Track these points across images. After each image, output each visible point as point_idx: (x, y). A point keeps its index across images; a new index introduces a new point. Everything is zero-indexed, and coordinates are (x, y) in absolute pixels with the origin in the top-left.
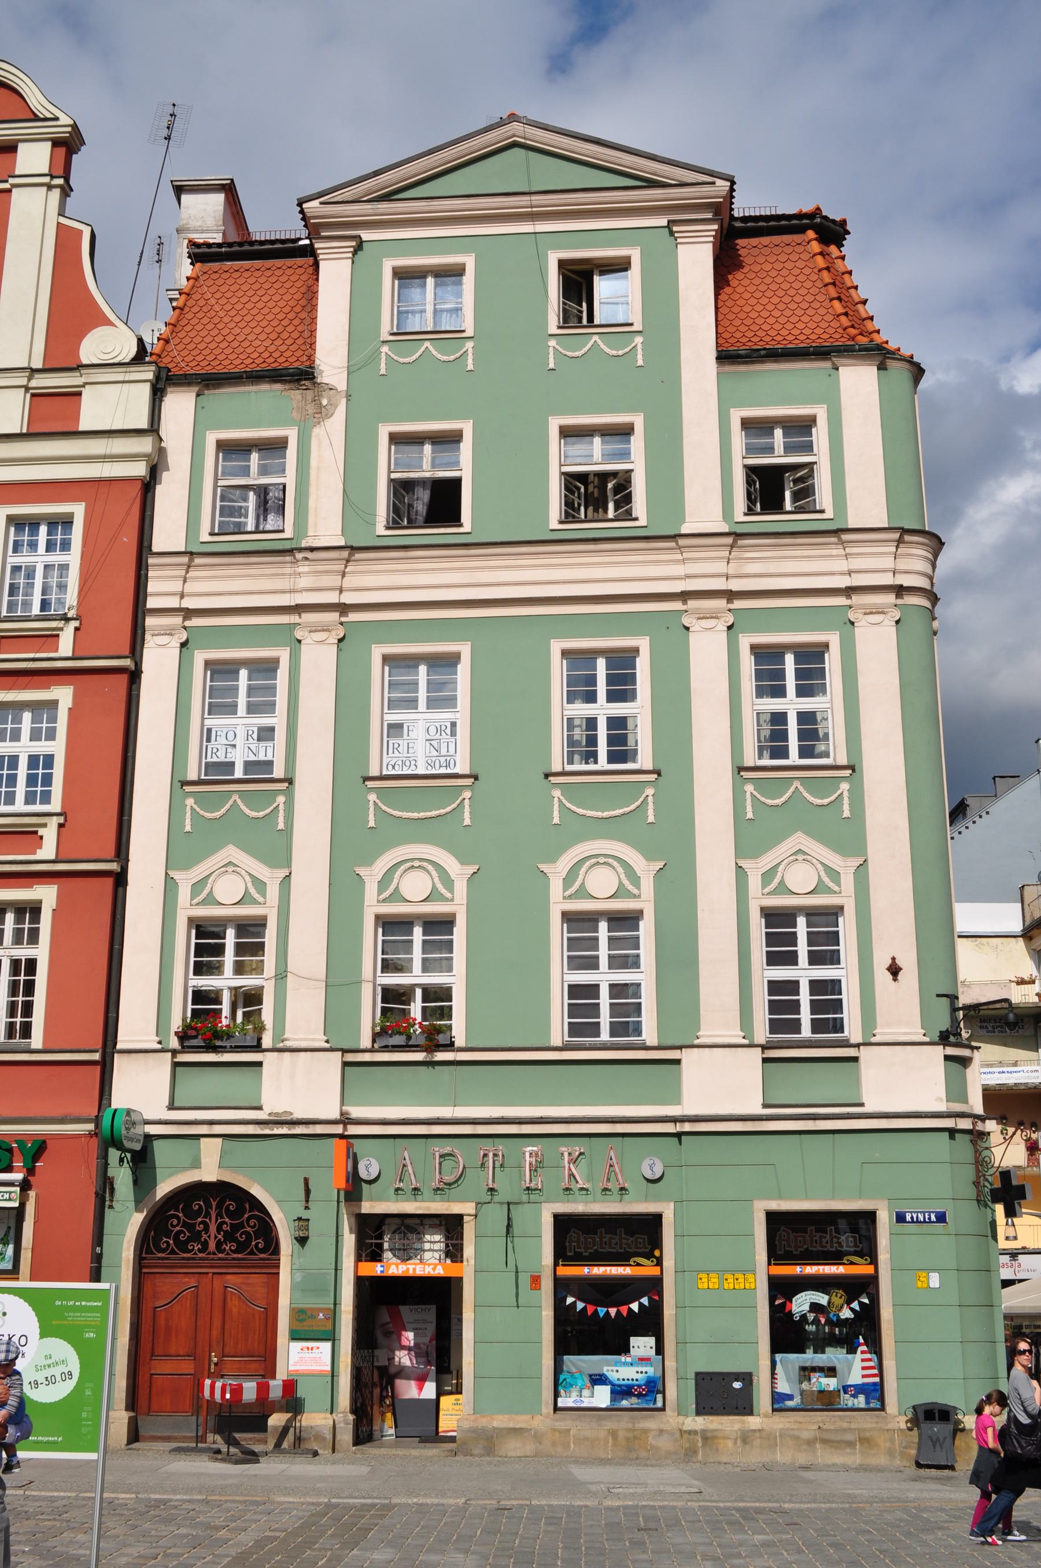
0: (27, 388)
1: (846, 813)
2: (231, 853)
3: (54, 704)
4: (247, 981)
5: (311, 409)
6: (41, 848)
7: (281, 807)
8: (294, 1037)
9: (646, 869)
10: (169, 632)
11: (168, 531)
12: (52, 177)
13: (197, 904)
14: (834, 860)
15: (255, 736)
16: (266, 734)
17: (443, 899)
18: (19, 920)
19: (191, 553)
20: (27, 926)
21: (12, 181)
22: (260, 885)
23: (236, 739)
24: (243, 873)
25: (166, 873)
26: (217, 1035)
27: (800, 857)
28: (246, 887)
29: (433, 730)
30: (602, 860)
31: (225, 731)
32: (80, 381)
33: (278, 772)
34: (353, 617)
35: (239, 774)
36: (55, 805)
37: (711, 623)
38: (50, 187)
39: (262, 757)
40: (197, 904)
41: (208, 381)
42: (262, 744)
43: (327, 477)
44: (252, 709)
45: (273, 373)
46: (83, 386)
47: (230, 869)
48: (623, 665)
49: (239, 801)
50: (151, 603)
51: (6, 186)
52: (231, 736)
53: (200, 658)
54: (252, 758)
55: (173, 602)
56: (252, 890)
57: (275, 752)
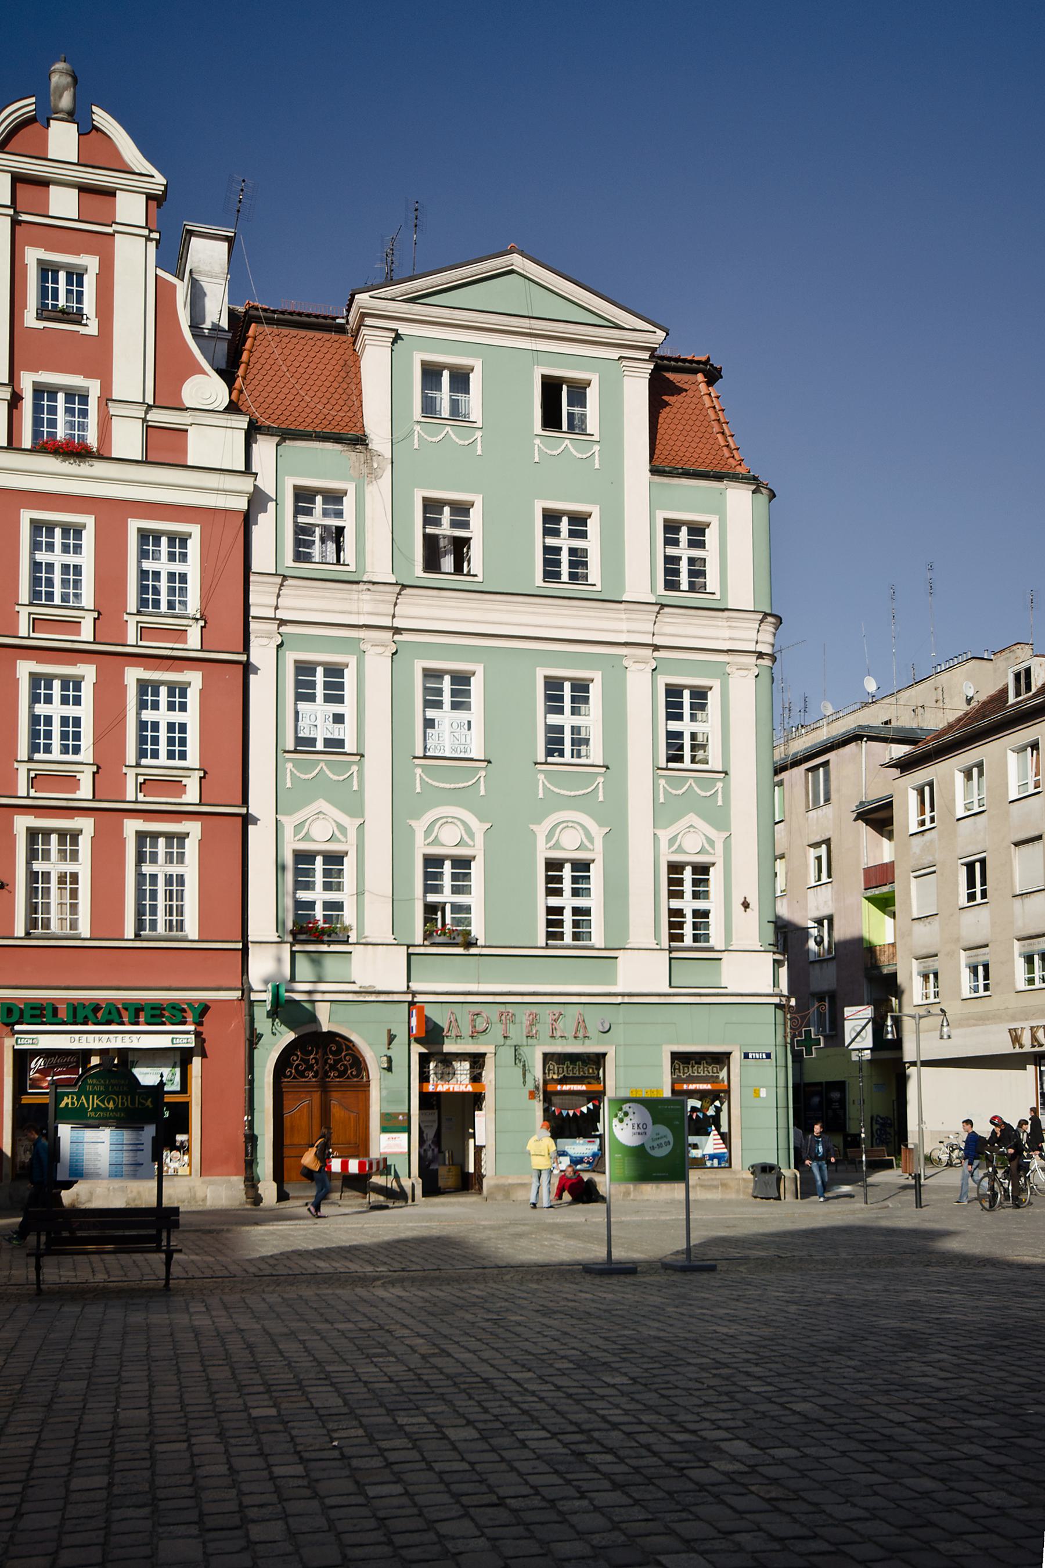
1: (720, 803)
4: (332, 896)
5: (365, 470)
6: (185, 793)
7: (355, 774)
9: (598, 832)
12: (151, 231)
14: (712, 833)
16: (339, 719)
17: (467, 845)
18: (169, 845)
20: (175, 850)
21: (115, 227)
22: (342, 829)
23: (316, 719)
27: (692, 830)
29: (455, 725)
30: (570, 824)
32: (189, 421)
34: (405, 637)
35: (320, 746)
36: (193, 759)
37: (642, 666)
38: (148, 239)
39: (336, 736)
41: (286, 435)
43: (378, 527)
45: (336, 436)
46: (191, 425)
47: (321, 816)
48: (581, 688)
50: (254, 612)
51: (110, 230)
52: (313, 718)
54: (329, 736)
57: (347, 732)
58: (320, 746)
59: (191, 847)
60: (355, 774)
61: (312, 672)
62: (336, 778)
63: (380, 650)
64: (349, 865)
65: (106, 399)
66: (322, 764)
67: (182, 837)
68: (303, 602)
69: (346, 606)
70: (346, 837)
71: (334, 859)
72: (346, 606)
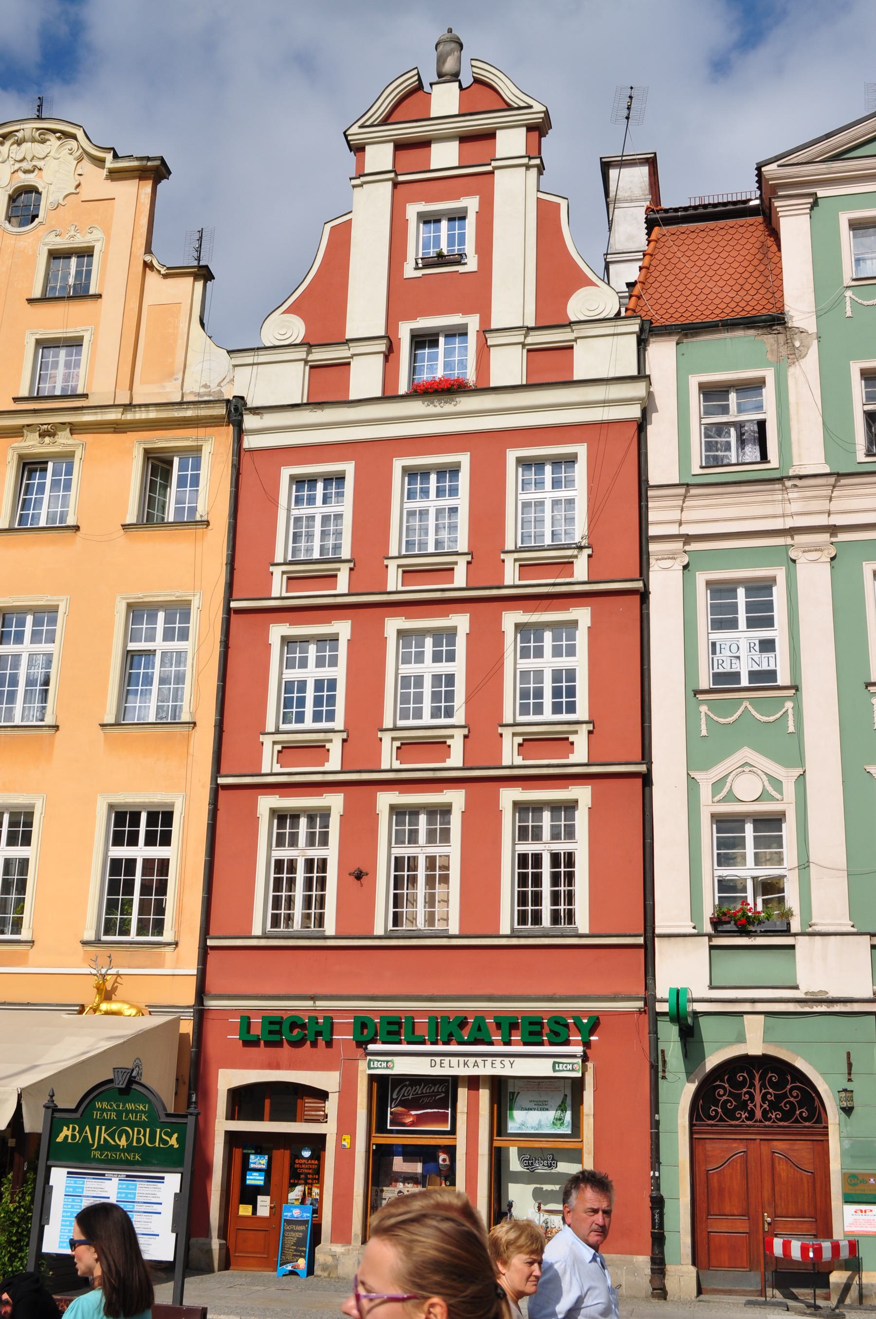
0: (524, 345)
2: (746, 754)
3: (574, 624)
7: (790, 712)
8: (821, 922)
10: (672, 556)
11: (662, 466)
13: (719, 801)
15: (757, 648)
16: (767, 646)
19: (688, 485)
23: (739, 649)
24: (759, 772)
25: (688, 774)
26: (750, 921)
28: (764, 786)
31: (728, 644)
33: (783, 679)
35: (745, 682)
39: (765, 667)
40: (719, 801)
42: (765, 655)
44: (752, 623)
47: (747, 769)
49: (750, 707)
50: (653, 531)
53: (701, 578)
54: (756, 668)
55: (673, 530)
56: (769, 788)
57: (779, 662)
58: (745, 682)
59: (581, 820)
60: (790, 712)
61: (733, 593)
62: (765, 719)
63: (814, 555)
64: (789, 831)
65: (485, 330)
66: (746, 704)
67: (571, 806)
68: (712, 514)
69: (769, 510)
70: (781, 793)
71: (769, 823)
72: (769, 510)
